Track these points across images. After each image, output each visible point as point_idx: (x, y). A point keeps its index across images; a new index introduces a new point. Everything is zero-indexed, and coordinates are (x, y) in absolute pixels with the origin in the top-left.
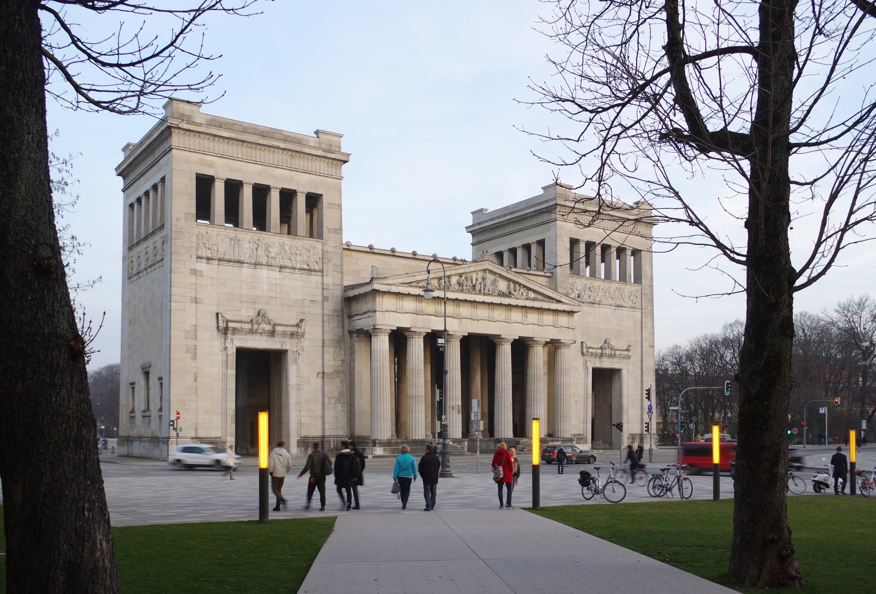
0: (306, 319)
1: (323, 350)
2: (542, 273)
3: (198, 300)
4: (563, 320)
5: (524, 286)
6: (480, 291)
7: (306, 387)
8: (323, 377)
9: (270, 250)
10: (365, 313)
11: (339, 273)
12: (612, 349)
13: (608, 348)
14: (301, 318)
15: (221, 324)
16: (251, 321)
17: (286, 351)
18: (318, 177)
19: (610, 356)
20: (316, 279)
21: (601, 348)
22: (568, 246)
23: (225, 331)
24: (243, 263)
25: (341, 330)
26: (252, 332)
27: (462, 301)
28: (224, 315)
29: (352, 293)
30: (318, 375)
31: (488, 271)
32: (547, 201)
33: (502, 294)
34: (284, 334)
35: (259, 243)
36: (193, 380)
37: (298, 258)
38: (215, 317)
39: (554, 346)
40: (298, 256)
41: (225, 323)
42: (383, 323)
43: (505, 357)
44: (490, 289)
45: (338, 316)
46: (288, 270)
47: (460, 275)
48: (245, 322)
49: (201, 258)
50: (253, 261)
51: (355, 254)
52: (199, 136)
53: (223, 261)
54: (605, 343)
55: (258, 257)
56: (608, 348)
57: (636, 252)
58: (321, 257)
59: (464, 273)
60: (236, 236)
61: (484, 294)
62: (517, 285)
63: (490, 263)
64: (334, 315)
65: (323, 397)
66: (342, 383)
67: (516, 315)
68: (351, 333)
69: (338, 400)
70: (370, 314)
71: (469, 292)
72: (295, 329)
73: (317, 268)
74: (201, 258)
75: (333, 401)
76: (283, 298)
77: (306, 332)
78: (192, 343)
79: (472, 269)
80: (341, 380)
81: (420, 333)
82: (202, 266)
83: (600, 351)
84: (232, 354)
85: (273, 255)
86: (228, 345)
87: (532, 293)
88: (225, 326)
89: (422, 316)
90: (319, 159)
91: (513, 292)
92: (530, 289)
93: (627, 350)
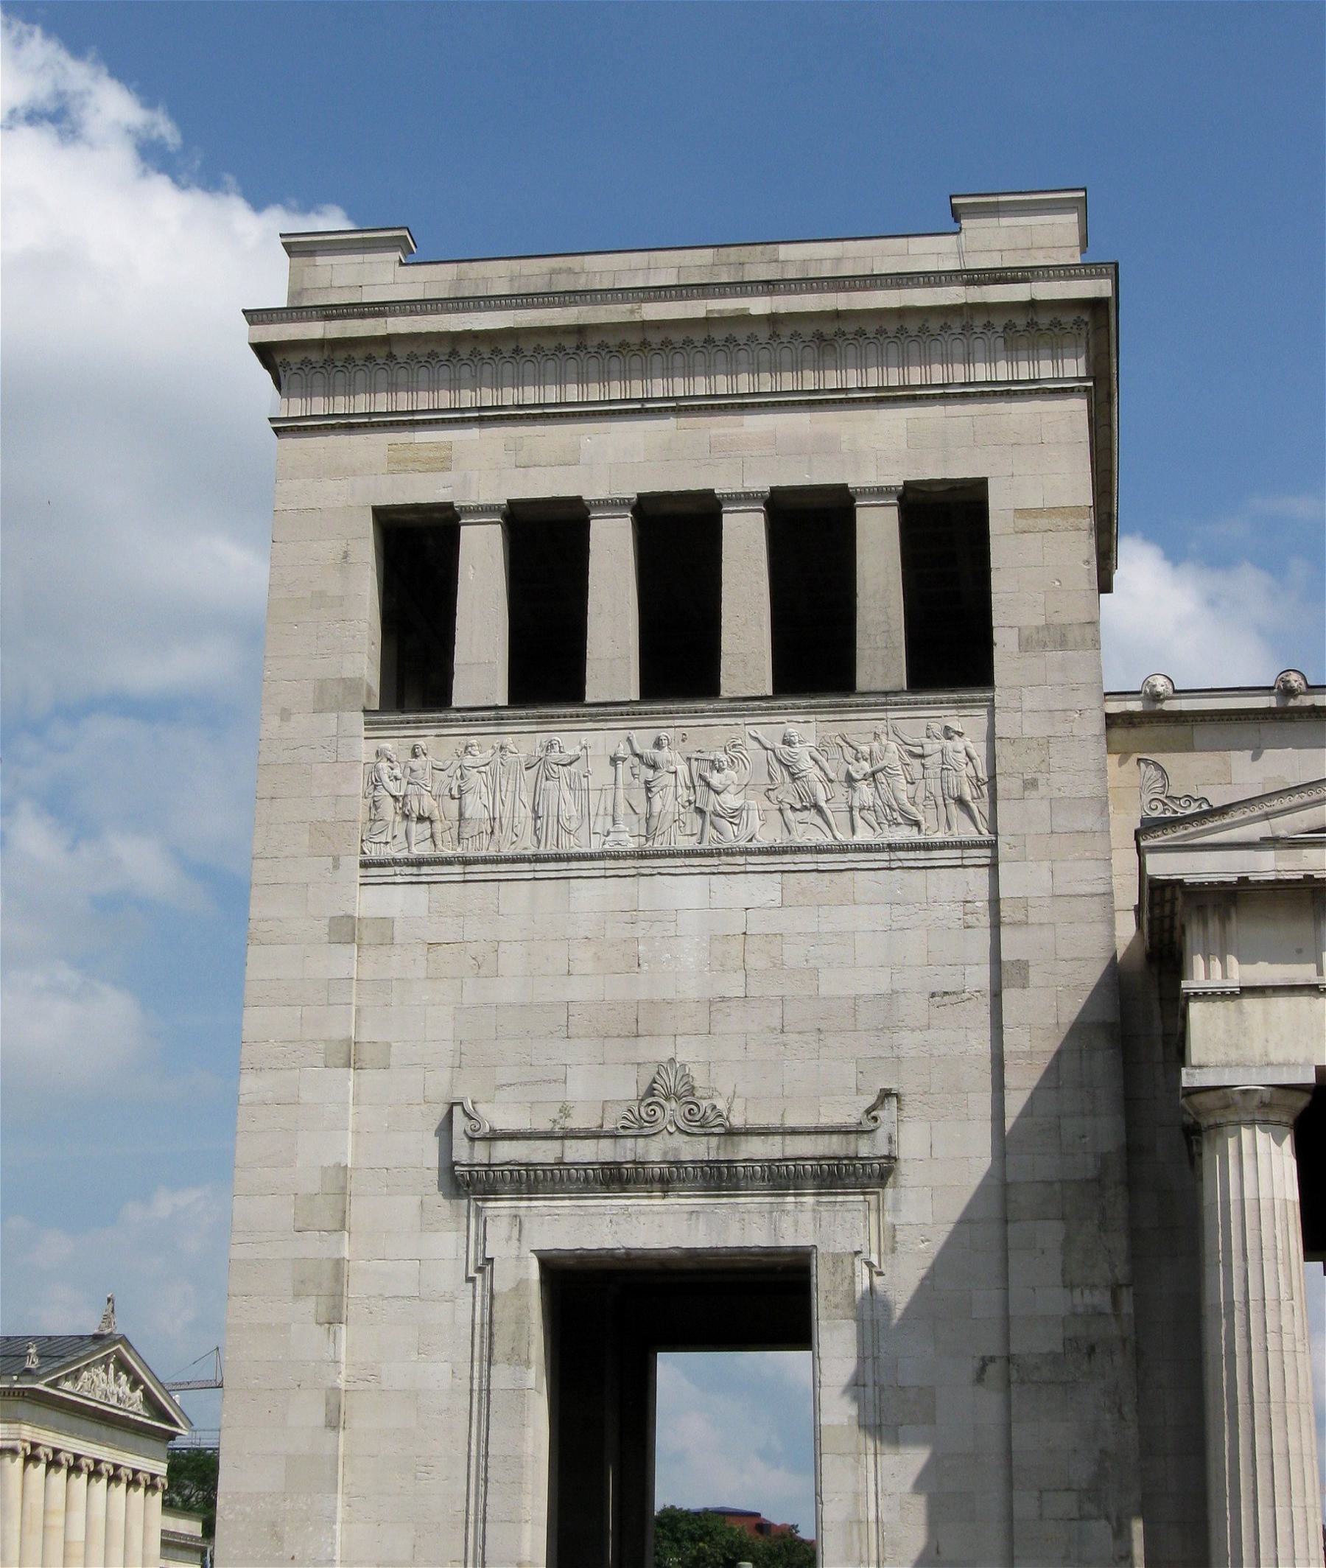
9: (715, 779)
30: (983, 1369)
35: (663, 755)
36: (321, 1420)
37: (865, 793)
40: (862, 786)
42: (1234, 1055)
50: (632, 845)
52: (391, 356)
55: (654, 823)
58: (983, 775)
60: (550, 746)
65: (1010, 1483)
76: (782, 998)
78: (315, 1247)
84: (516, 1289)
85: (730, 800)
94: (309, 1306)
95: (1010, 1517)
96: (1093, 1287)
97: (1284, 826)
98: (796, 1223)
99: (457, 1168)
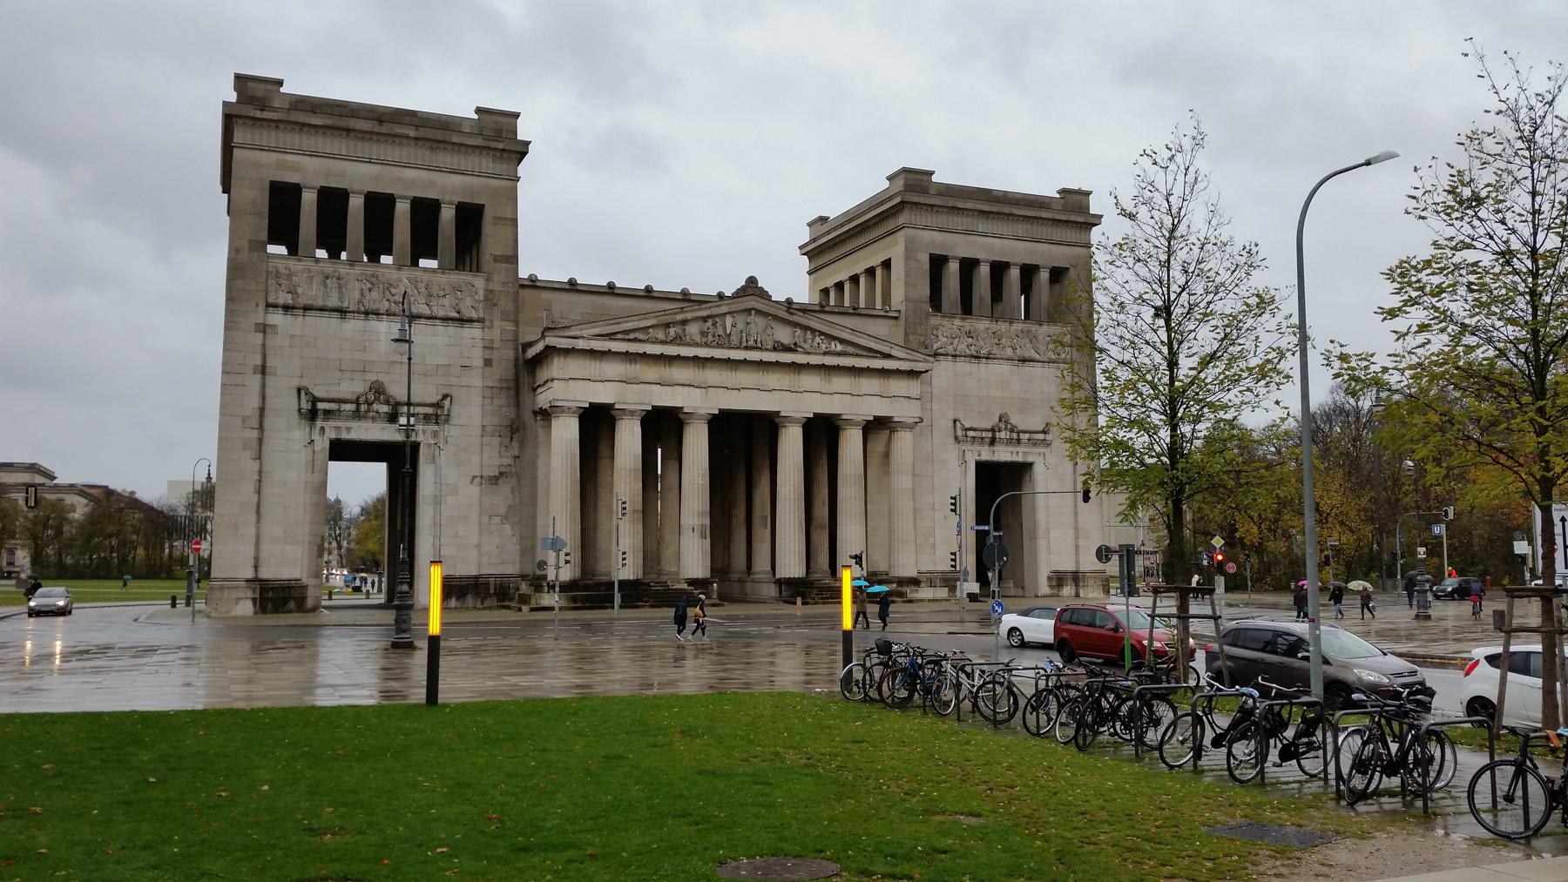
0: (455, 394)
2: (882, 313)
3: (268, 370)
4: (899, 386)
5: (822, 333)
6: (741, 343)
7: (450, 499)
9: (393, 291)
11: (512, 324)
12: (1012, 431)
13: (1006, 429)
14: (445, 391)
16: (358, 398)
18: (476, 178)
19: (1010, 442)
20: (473, 333)
21: (993, 430)
22: (927, 266)
23: (312, 415)
24: (346, 312)
25: (513, 410)
26: (357, 415)
27: (706, 359)
29: (531, 352)
30: (473, 480)
31: (753, 312)
32: (890, 198)
33: (780, 347)
38: (296, 395)
39: (877, 427)
43: (791, 445)
44: (759, 340)
45: (509, 389)
46: (423, 321)
47: (705, 319)
49: (275, 306)
51: (546, 295)
53: (312, 309)
54: (1000, 420)
56: (1006, 429)
57: (1057, 274)
59: (709, 317)
61: (746, 348)
62: (809, 332)
63: (758, 299)
66: (513, 493)
67: (810, 381)
69: (506, 518)
70: (549, 384)
71: (719, 346)
72: (429, 410)
73: (474, 315)
74: (275, 306)
75: (497, 520)
77: (454, 412)
79: (724, 309)
80: (512, 488)
81: (632, 413)
82: (276, 318)
83: (990, 435)
86: (316, 436)
87: (838, 345)
89: (634, 386)
90: (478, 151)
91: (800, 342)
92: (835, 338)
93: (1044, 432)
94: (249, 454)
95: (480, 524)
97: (585, 333)
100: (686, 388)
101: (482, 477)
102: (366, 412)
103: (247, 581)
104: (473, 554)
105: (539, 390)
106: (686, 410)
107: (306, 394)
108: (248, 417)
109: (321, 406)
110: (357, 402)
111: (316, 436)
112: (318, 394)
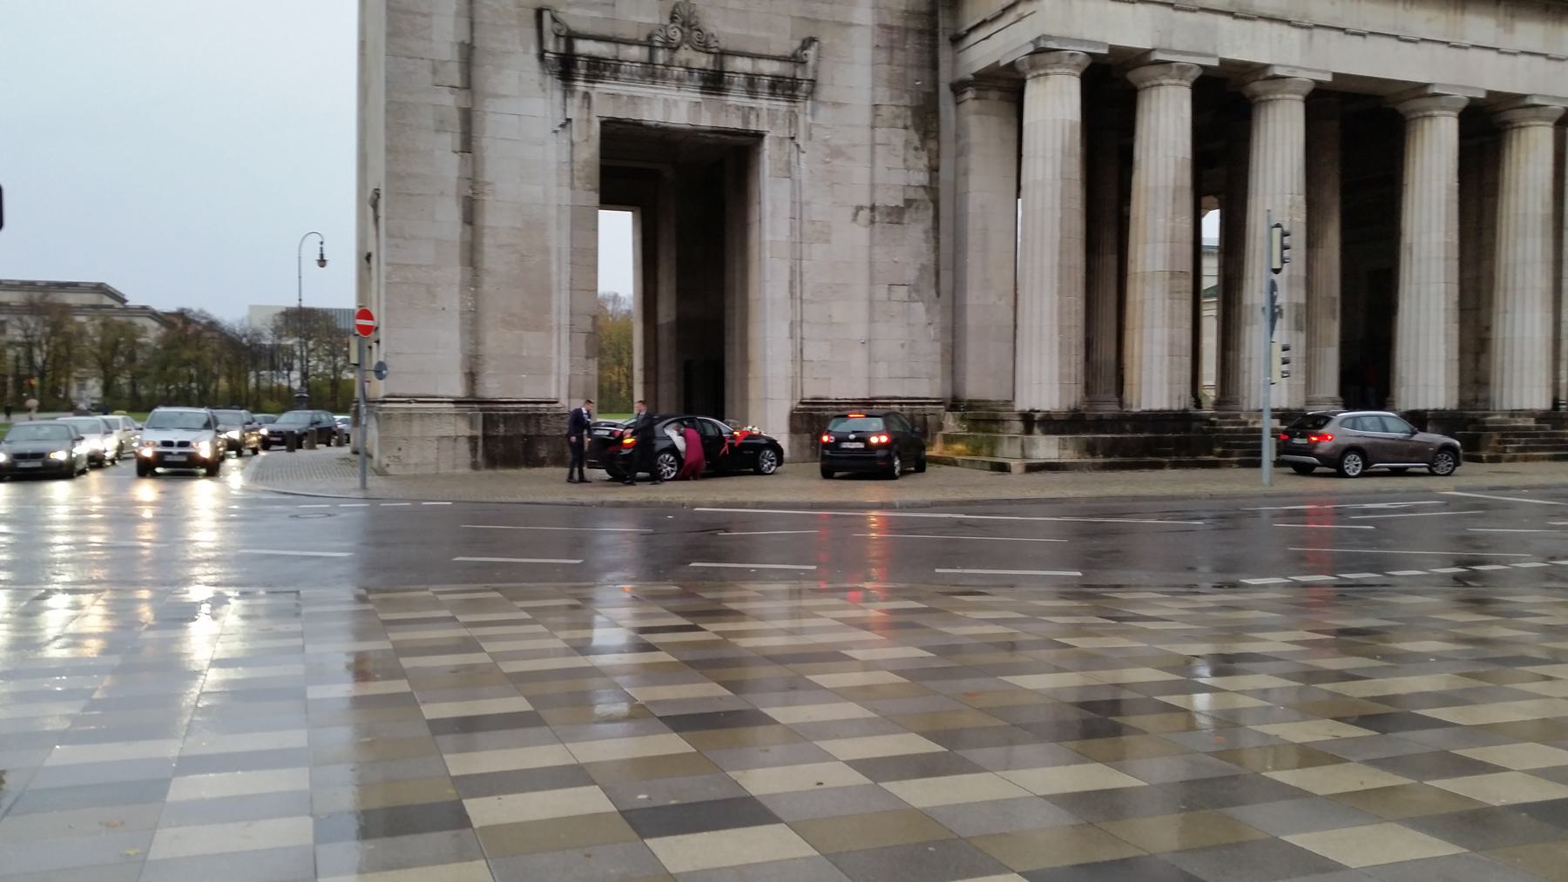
1: (873, 138)
8: (872, 222)
10: (1006, 10)
14: (806, 35)
15: (550, 45)
16: (650, 37)
17: (759, 136)
23: (565, 67)
26: (651, 73)
28: (560, 16)
34: (752, 81)
41: (562, 42)
45: (920, 32)
48: (629, 43)
64: (907, 30)
68: (958, 88)
88: (562, 49)
96: (920, 170)
98: (758, 116)
99: (547, 55)
100: (1276, 26)
101: (873, 208)
102: (667, 65)
103: (457, 402)
104: (858, 358)
105: (974, 37)
106: (1279, 72)
107: (555, 20)
108: (444, 63)
109: (582, 47)
110: (649, 44)
111: (575, 110)
112: (577, 26)
